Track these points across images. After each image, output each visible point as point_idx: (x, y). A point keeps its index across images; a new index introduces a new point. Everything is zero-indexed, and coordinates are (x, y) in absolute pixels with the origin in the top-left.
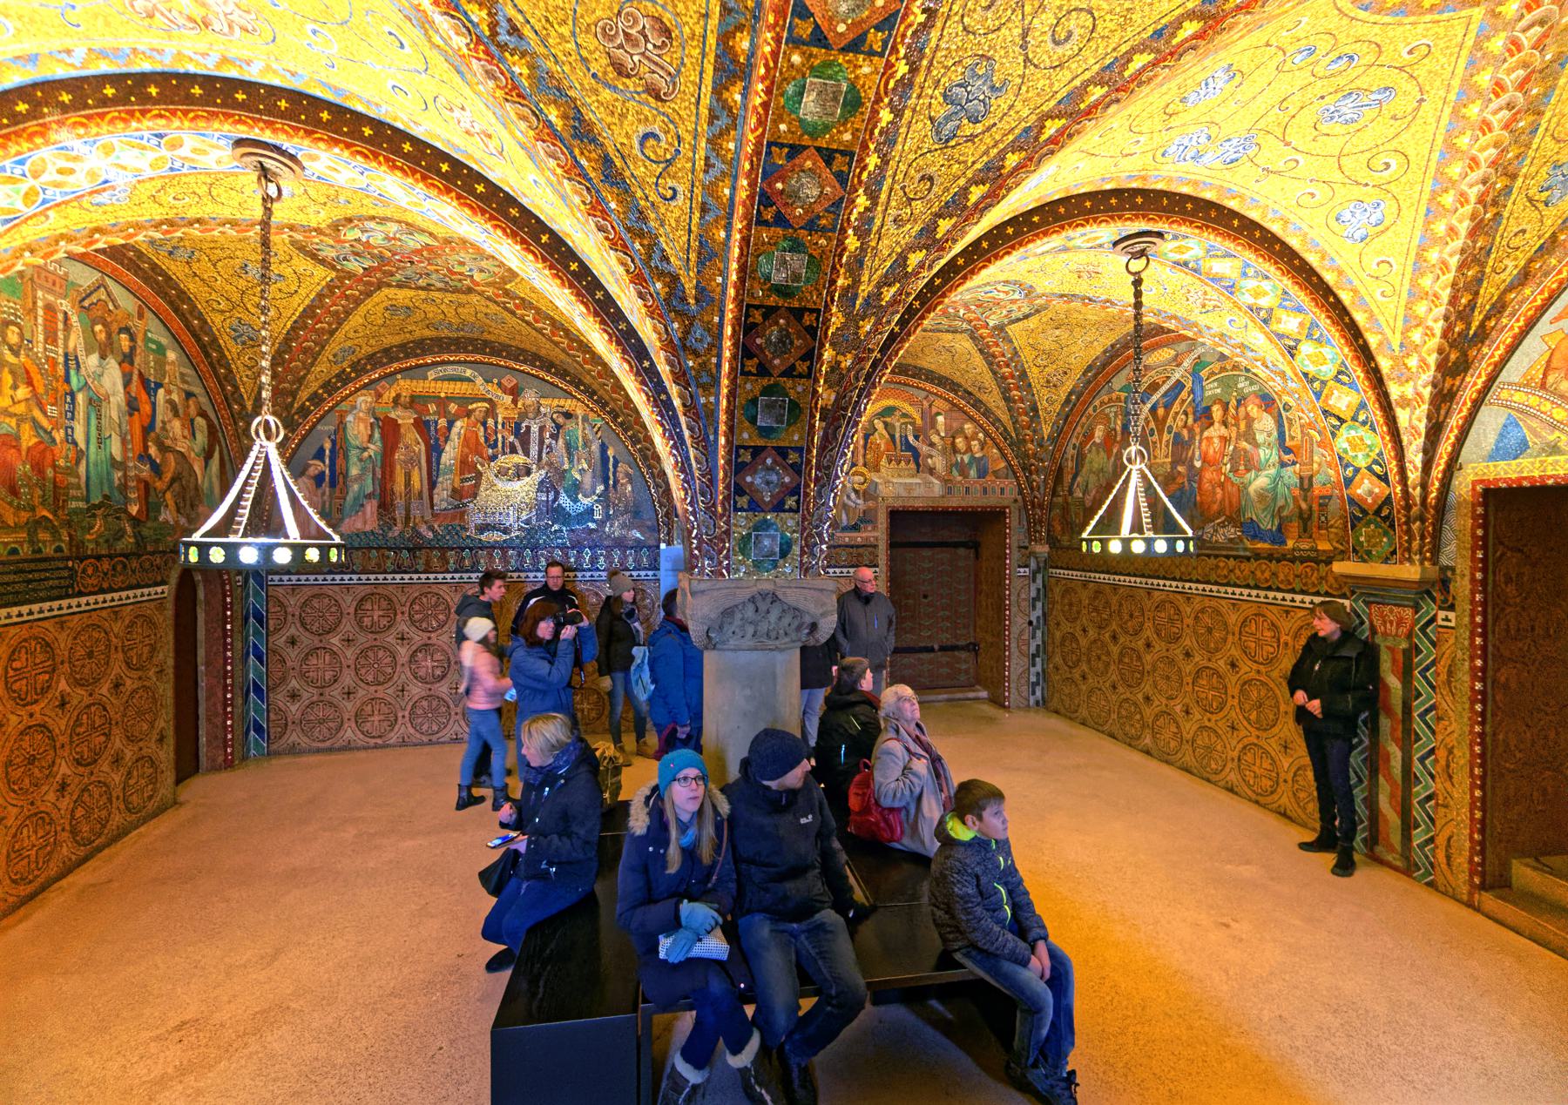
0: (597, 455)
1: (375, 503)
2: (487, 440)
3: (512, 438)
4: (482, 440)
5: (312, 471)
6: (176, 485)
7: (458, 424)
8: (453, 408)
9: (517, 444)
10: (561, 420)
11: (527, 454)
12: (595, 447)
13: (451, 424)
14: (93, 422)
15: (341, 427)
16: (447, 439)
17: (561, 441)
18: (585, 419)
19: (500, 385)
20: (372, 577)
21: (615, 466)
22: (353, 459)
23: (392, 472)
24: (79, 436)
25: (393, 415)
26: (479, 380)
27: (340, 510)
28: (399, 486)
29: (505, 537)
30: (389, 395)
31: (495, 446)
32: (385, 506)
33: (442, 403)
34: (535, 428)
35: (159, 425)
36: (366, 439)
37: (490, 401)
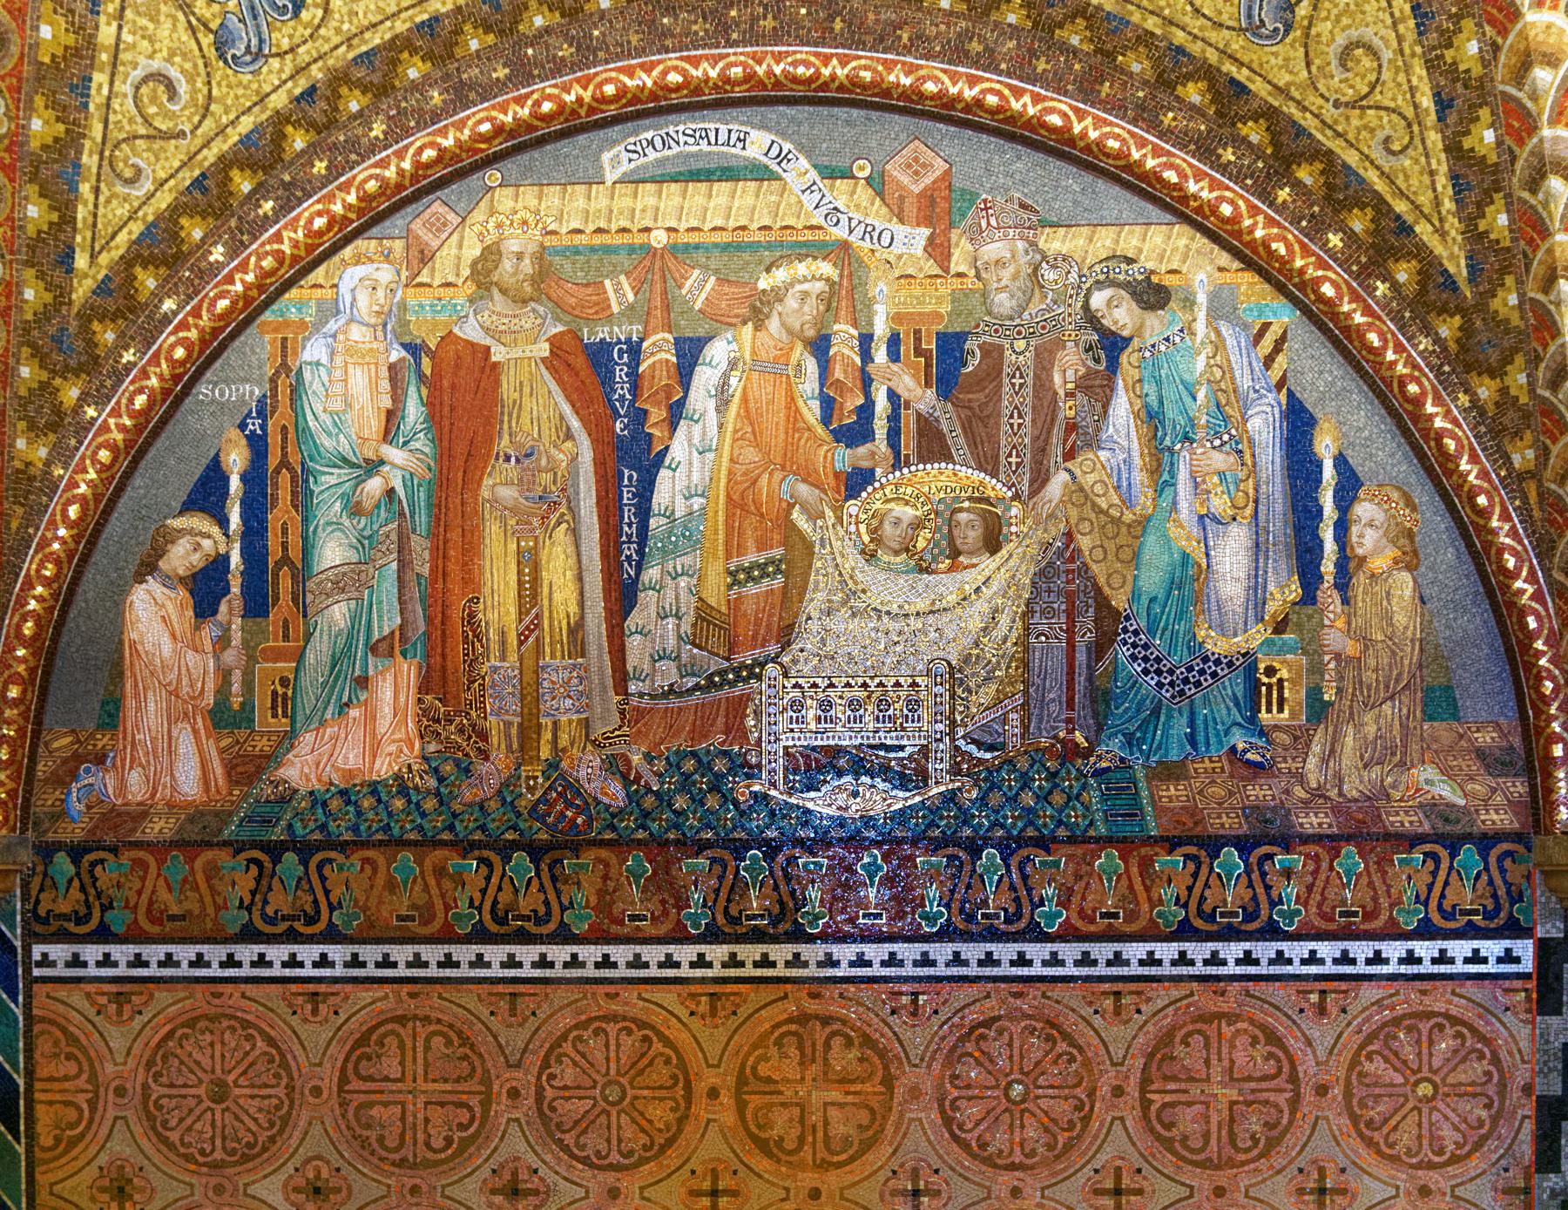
1: (408, 671)
2: (828, 406)
3: (924, 399)
4: (811, 411)
5: (182, 557)
7: (718, 351)
8: (698, 288)
9: (948, 420)
11: (988, 464)
12: (1264, 424)
13: (689, 354)
15: (287, 381)
16: (676, 413)
17: (1122, 408)
18: (1222, 308)
19: (878, 184)
20: (402, 953)
22: (329, 508)
23: (472, 547)
25: (471, 331)
26: (800, 171)
27: (282, 703)
28: (500, 606)
29: (902, 799)
30: (457, 252)
31: (857, 433)
32: (447, 682)
33: (656, 265)
34: (1019, 354)
36: (375, 425)
37: (842, 252)
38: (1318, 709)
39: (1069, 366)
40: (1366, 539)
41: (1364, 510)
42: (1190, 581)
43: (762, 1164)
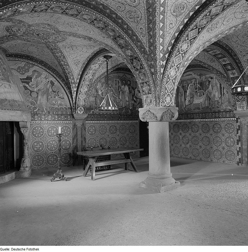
0: (219, 87)
6: (140, 104)
10: (210, 79)
12: (218, 85)
13: (188, 85)
14: (123, 95)
21: (223, 89)
24: (121, 97)
35: (136, 94)
38: (222, 103)
39: (207, 83)
40: (225, 92)
41: (224, 90)
42: (214, 95)
43: (192, 132)
